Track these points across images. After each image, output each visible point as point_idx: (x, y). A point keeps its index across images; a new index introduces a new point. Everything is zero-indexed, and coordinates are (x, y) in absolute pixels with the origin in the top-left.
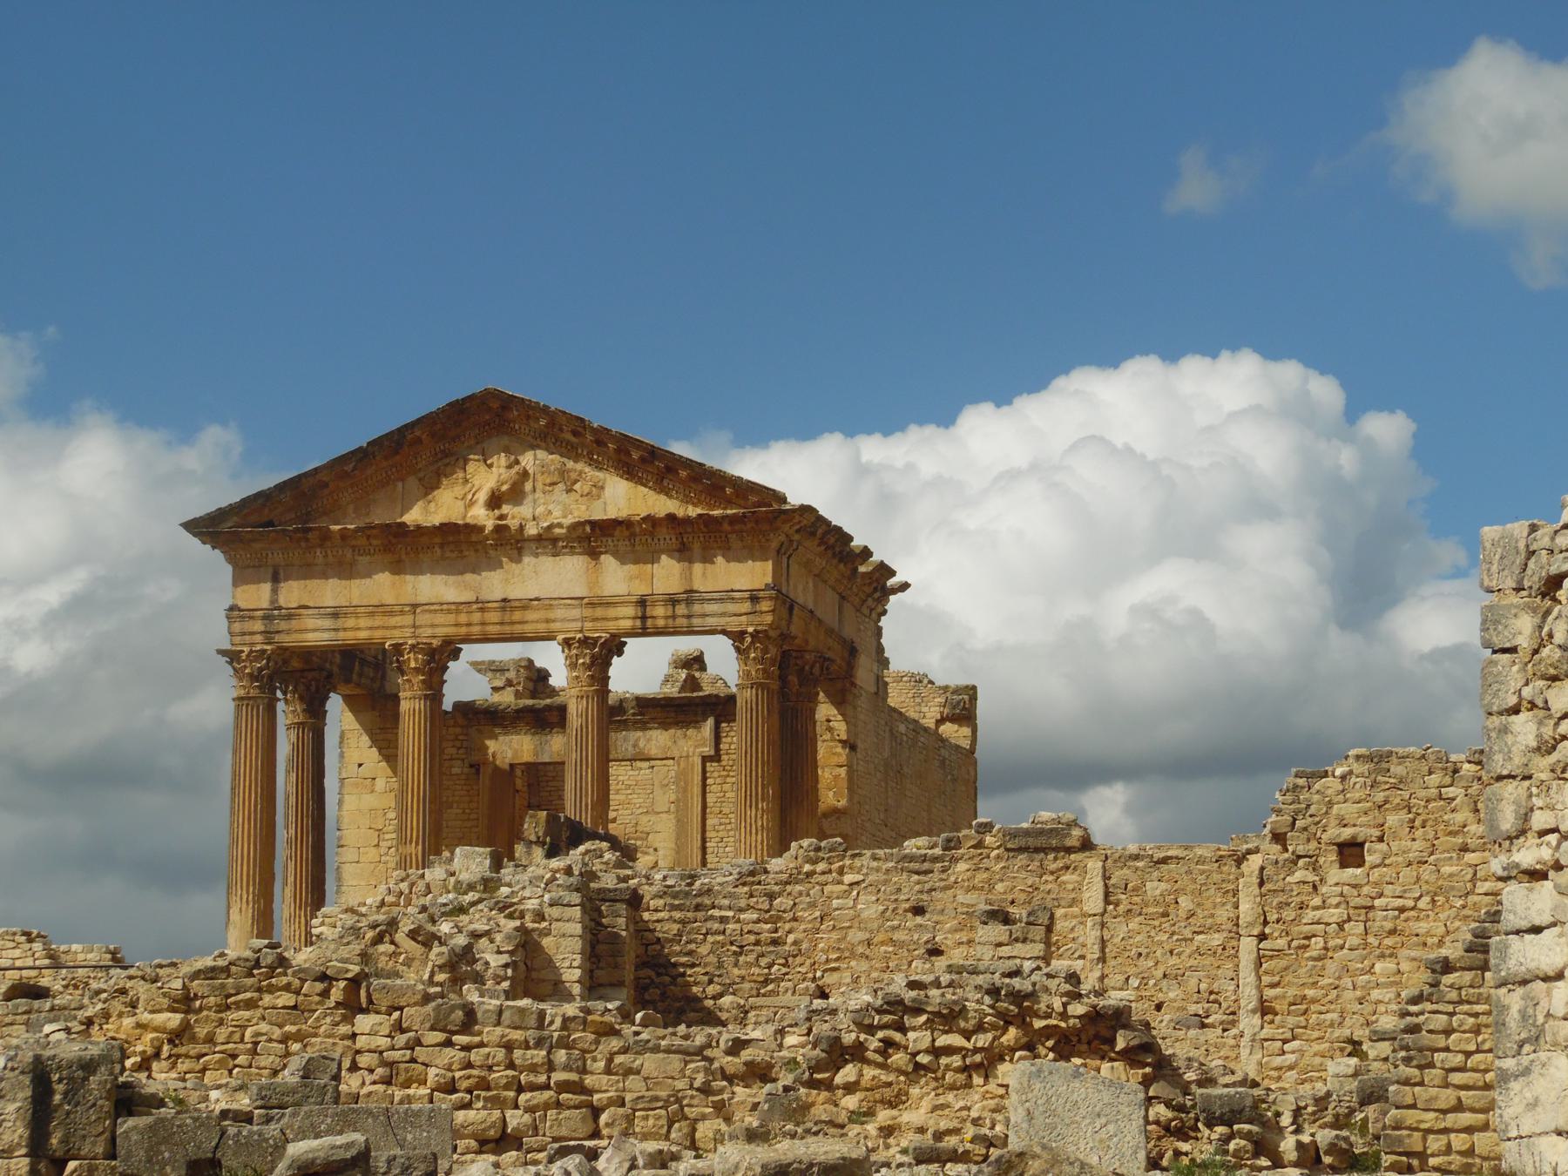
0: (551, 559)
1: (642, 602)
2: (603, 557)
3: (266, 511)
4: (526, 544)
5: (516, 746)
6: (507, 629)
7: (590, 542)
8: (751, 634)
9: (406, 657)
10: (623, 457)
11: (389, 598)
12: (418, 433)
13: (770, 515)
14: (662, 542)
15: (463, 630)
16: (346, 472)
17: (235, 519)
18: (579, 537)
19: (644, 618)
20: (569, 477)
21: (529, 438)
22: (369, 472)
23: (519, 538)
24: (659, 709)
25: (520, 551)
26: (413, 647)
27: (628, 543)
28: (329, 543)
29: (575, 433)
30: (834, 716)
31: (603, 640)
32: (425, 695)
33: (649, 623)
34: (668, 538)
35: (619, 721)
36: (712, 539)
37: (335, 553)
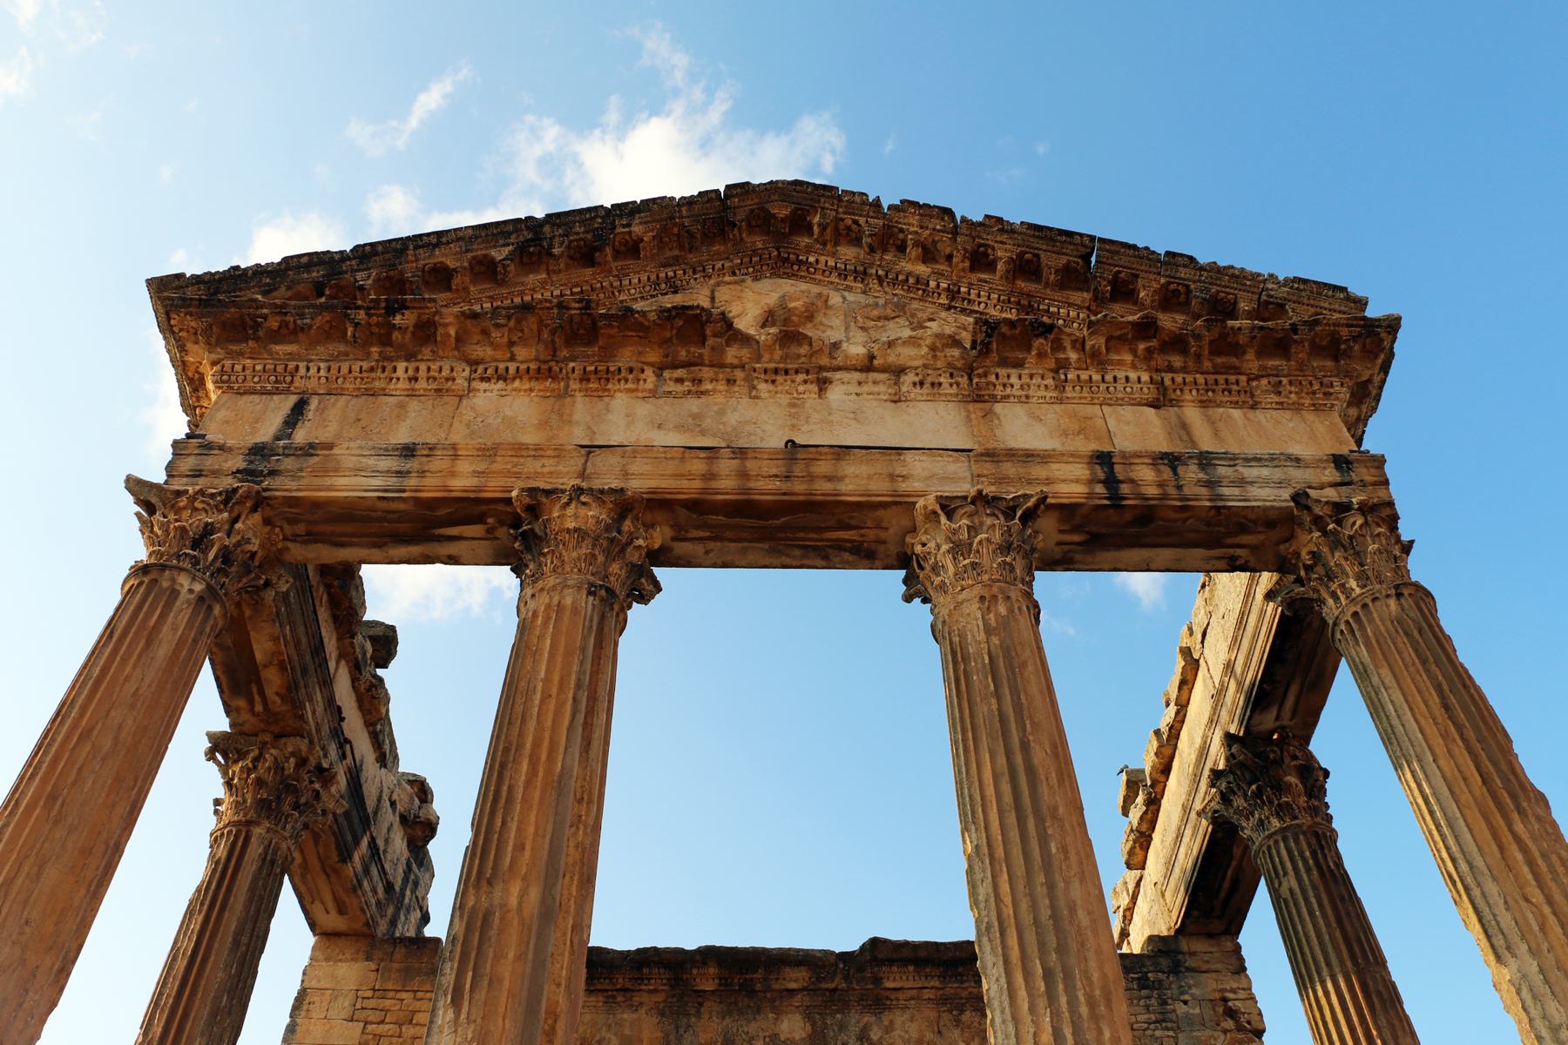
0: (893, 404)
1: (1103, 459)
2: (998, 408)
3: (323, 300)
4: (838, 375)
5: (627, 1032)
6: (799, 487)
7: (971, 380)
8: (1365, 509)
9: (556, 514)
10: (1021, 284)
11: (529, 438)
12: (637, 229)
13: (1344, 332)
14: (1120, 387)
15: (697, 484)
16: (492, 260)
17: (259, 297)
18: (950, 365)
19: (1111, 482)
20: (913, 315)
21: (834, 278)
22: (532, 279)
23: (825, 361)
24: (911, 968)
25: (823, 384)
26: (579, 491)
27: (1050, 382)
28: (426, 352)
29: (928, 255)
30: (1233, 991)
31: (1033, 500)
32: (591, 585)
33: (1125, 489)
34: (1133, 375)
35: (835, 990)
36: (1221, 387)
37: (432, 373)
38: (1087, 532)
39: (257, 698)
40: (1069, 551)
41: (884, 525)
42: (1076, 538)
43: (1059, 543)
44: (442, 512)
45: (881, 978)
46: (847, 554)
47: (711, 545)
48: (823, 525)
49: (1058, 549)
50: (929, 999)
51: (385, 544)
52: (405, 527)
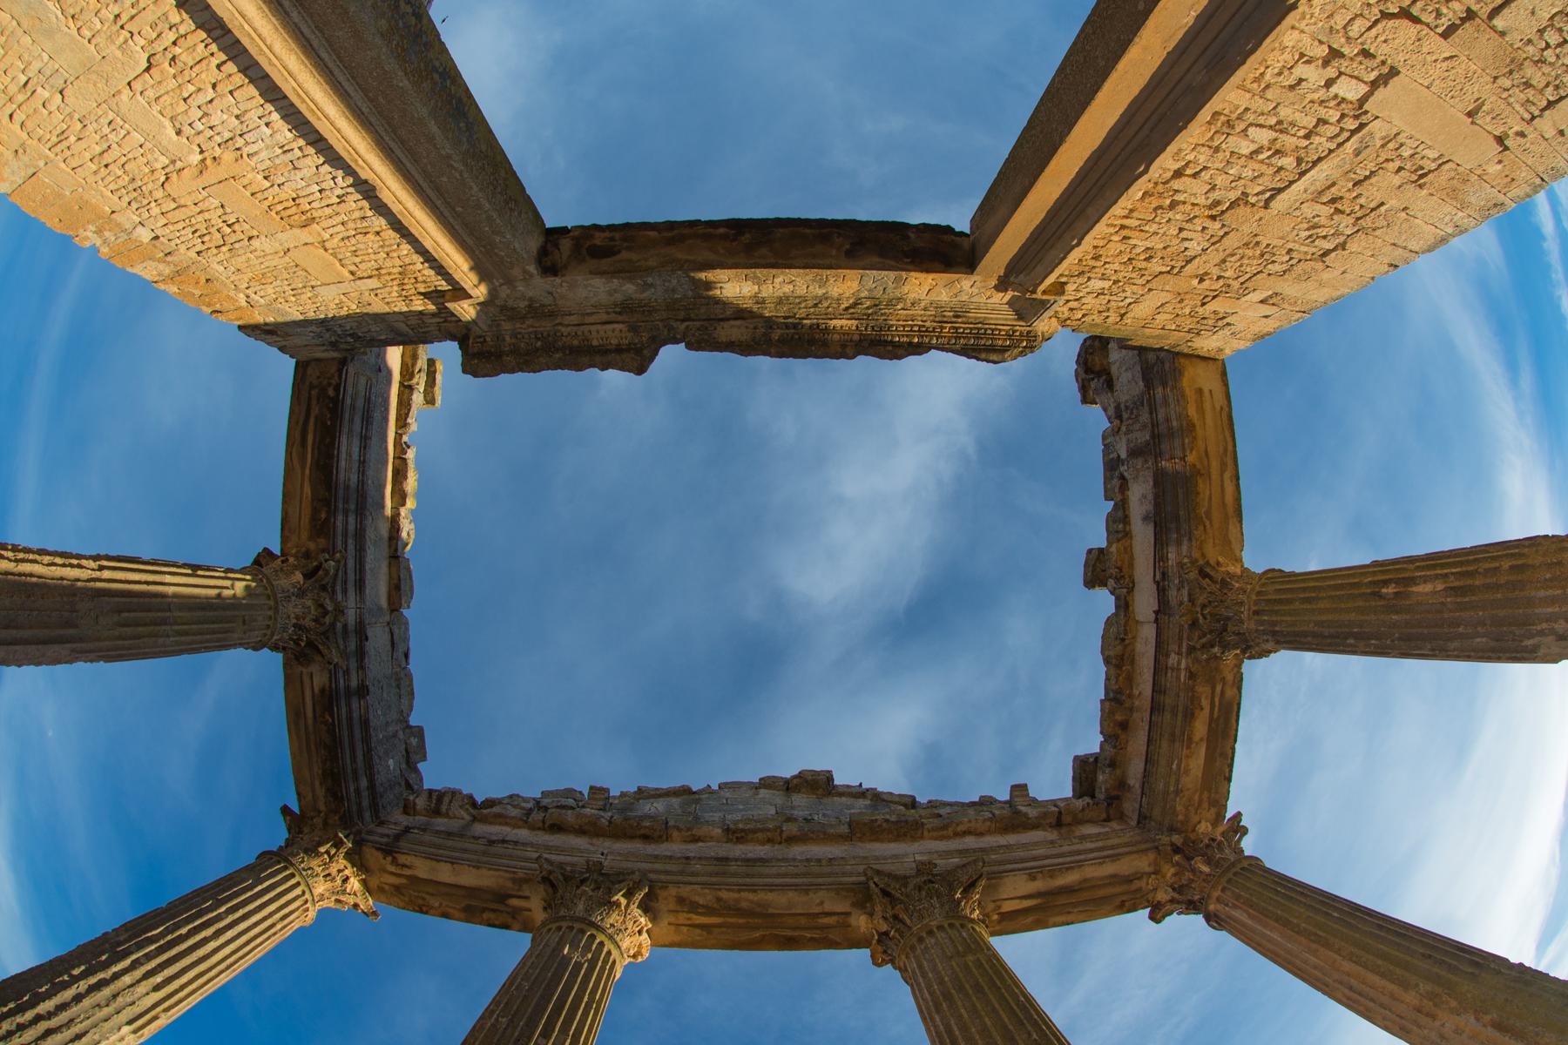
24: (595, 343)
38: (506, 905)
39: (1217, 700)
40: (519, 890)
41: (673, 928)
42: (514, 902)
43: (527, 898)
44: (1030, 919)
45: (629, 331)
46: (701, 902)
47: (817, 910)
48: (724, 929)
49: (527, 893)
50: (570, 315)
51: (1080, 883)
52: (1062, 900)
